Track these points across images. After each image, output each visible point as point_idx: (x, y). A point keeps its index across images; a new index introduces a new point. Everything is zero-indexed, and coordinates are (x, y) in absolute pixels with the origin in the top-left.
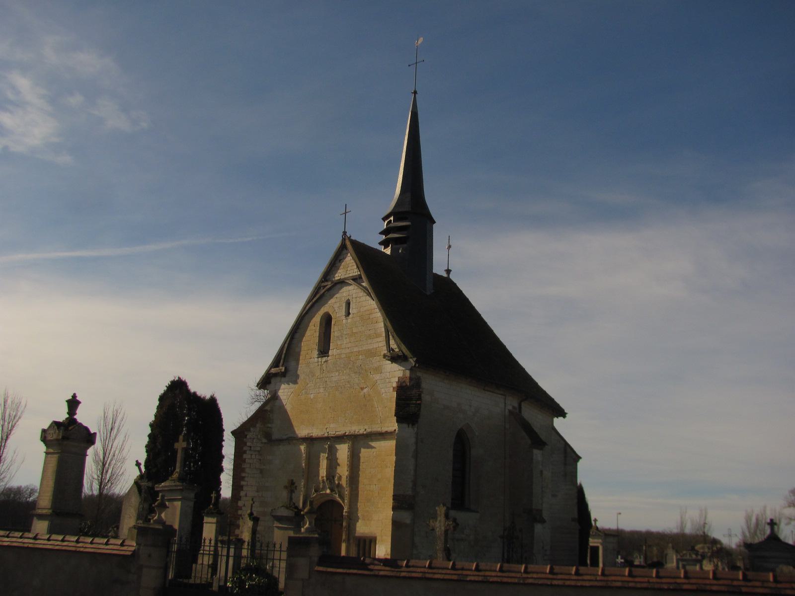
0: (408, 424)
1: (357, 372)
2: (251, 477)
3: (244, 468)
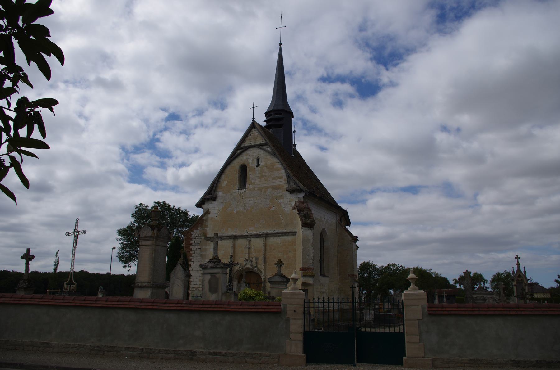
0: (309, 228)
1: (266, 198)
2: (195, 259)
3: (191, 254)
